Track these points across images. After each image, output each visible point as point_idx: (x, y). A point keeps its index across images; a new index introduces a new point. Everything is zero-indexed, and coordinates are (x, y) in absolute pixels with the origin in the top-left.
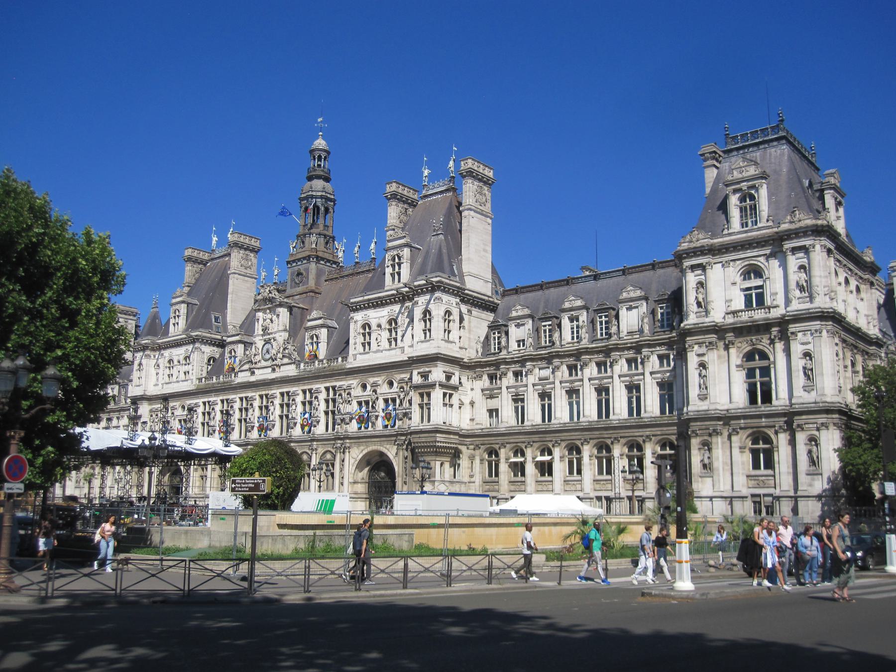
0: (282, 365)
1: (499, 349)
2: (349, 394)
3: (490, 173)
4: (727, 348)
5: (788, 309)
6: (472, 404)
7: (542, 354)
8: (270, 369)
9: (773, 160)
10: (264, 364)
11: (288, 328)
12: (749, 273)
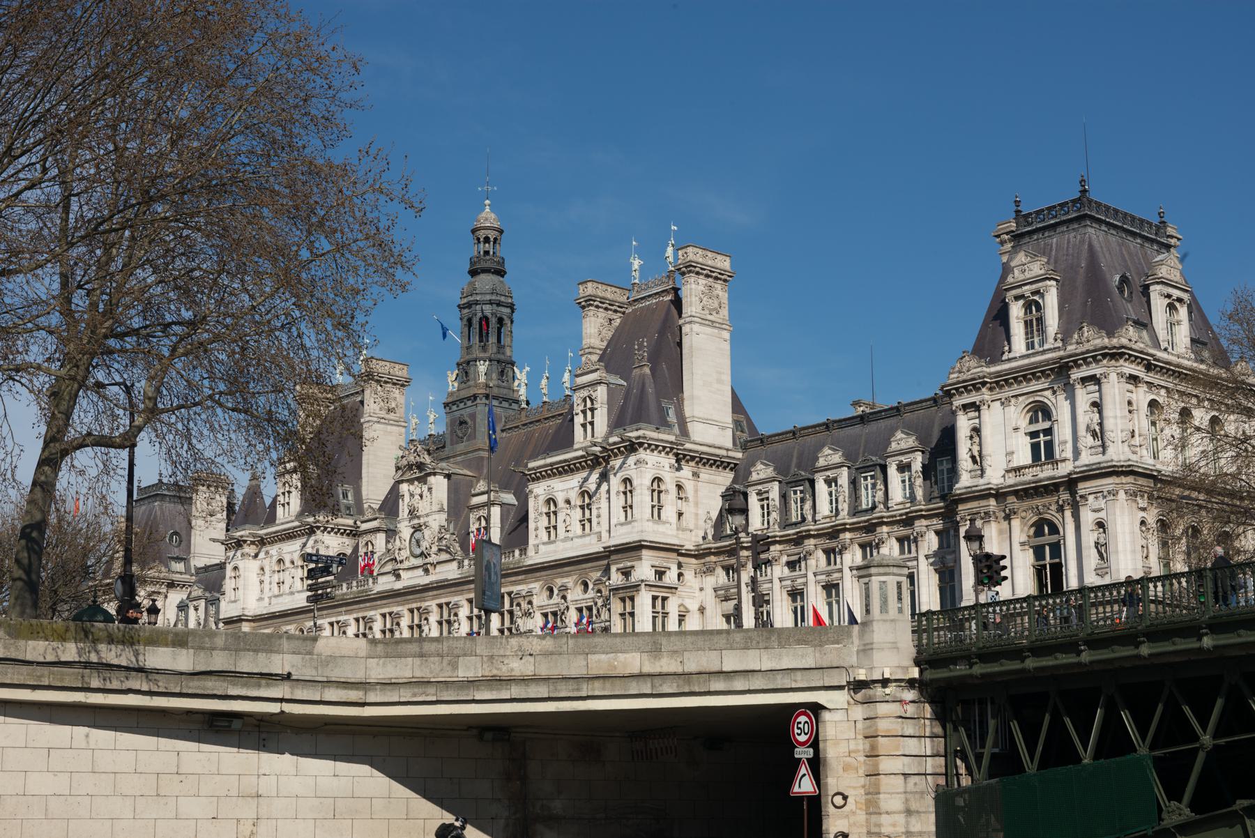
0: (438, 563)
2: (530, 603)
3: (724, 263)
4: (1008, 518)
5: (1077, 463)
6: (702, 610)
7: (789, 535)
8: (420, 572)
9: (1071, 251)
11: (445, 507)
12: (1036, 412)
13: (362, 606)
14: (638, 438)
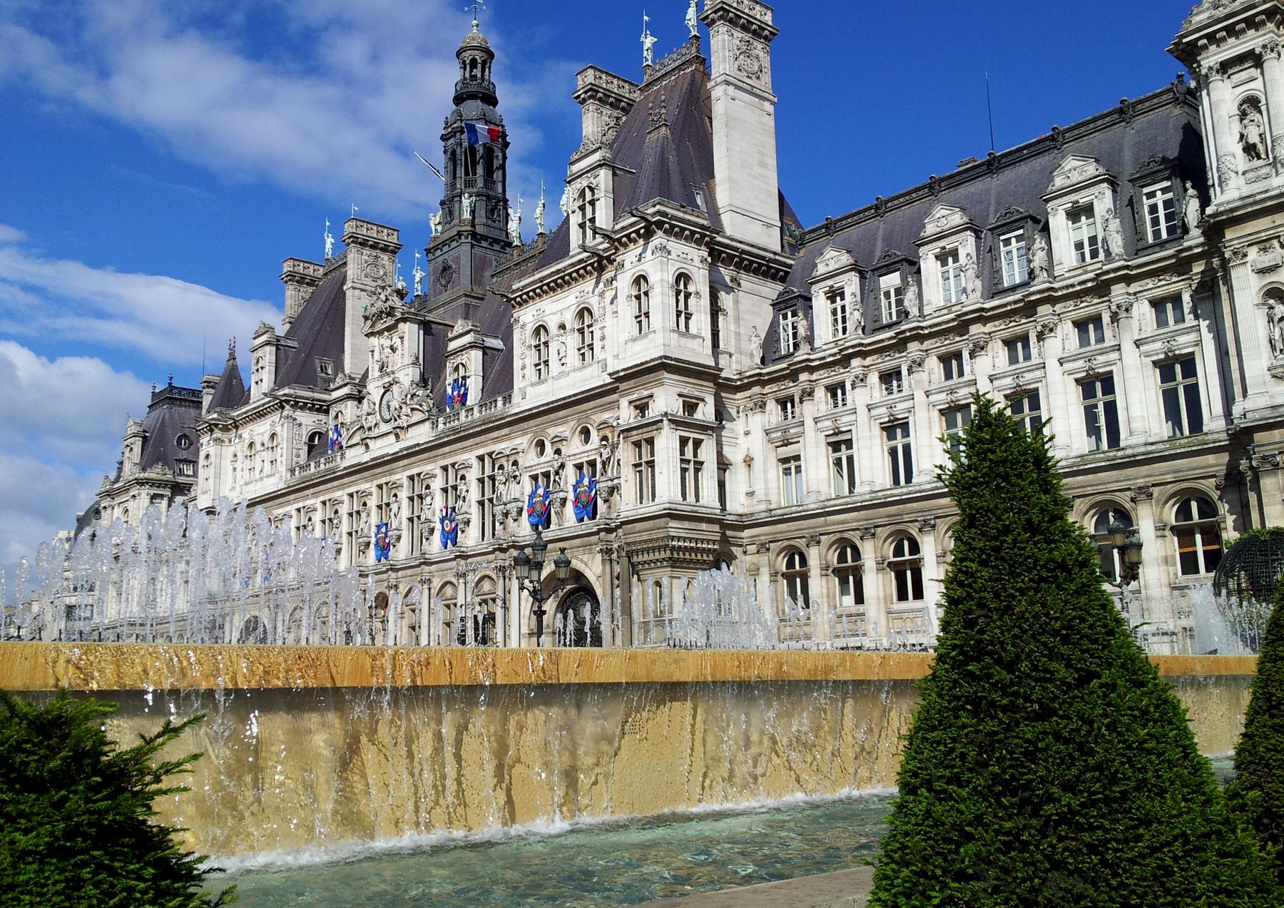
0: (409, 426)
1: (796, 346)
2: (515, 463)
6: (748, 461)
7: (883, 341)
8: (392, 438)
10: (384, 428)
13: (329, 485)
14: (659, 213)
